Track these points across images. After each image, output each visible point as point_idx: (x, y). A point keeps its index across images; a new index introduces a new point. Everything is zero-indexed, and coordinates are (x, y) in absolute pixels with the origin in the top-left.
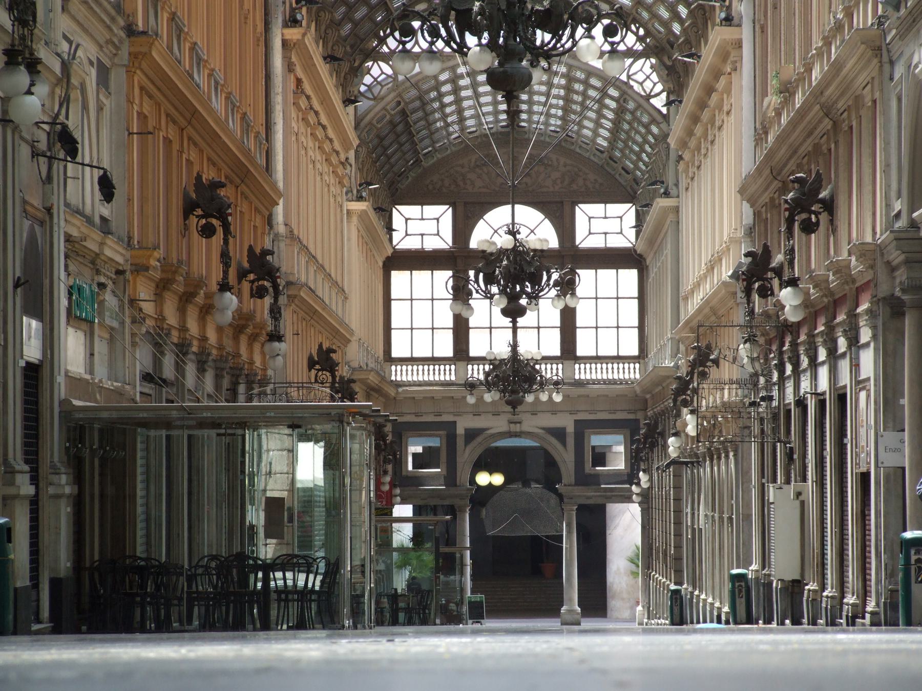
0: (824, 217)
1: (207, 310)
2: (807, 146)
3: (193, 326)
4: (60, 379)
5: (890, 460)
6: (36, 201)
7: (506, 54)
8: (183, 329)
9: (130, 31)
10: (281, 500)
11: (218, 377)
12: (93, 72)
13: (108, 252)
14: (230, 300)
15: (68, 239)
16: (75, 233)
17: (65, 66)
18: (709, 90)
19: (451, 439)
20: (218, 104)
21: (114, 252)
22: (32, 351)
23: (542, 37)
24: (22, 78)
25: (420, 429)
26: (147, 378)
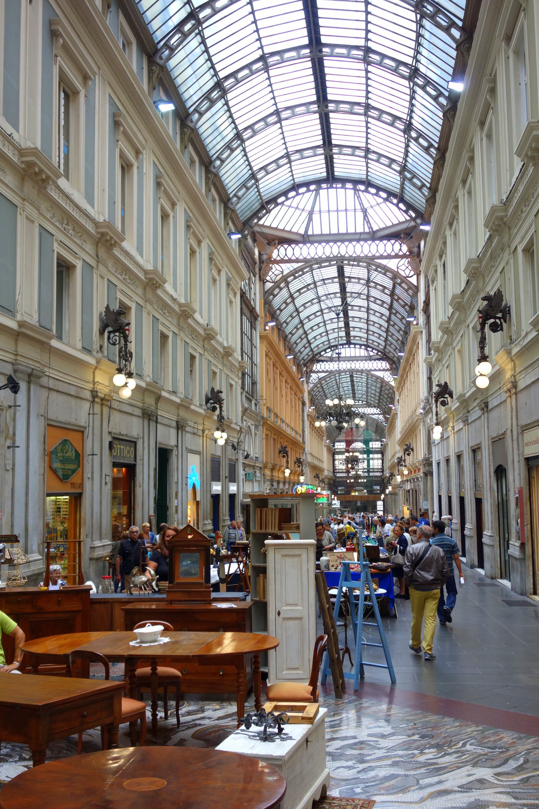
0: (412, 452)
7: (340, 422)
12: (253, 427)
17: (241, 428)
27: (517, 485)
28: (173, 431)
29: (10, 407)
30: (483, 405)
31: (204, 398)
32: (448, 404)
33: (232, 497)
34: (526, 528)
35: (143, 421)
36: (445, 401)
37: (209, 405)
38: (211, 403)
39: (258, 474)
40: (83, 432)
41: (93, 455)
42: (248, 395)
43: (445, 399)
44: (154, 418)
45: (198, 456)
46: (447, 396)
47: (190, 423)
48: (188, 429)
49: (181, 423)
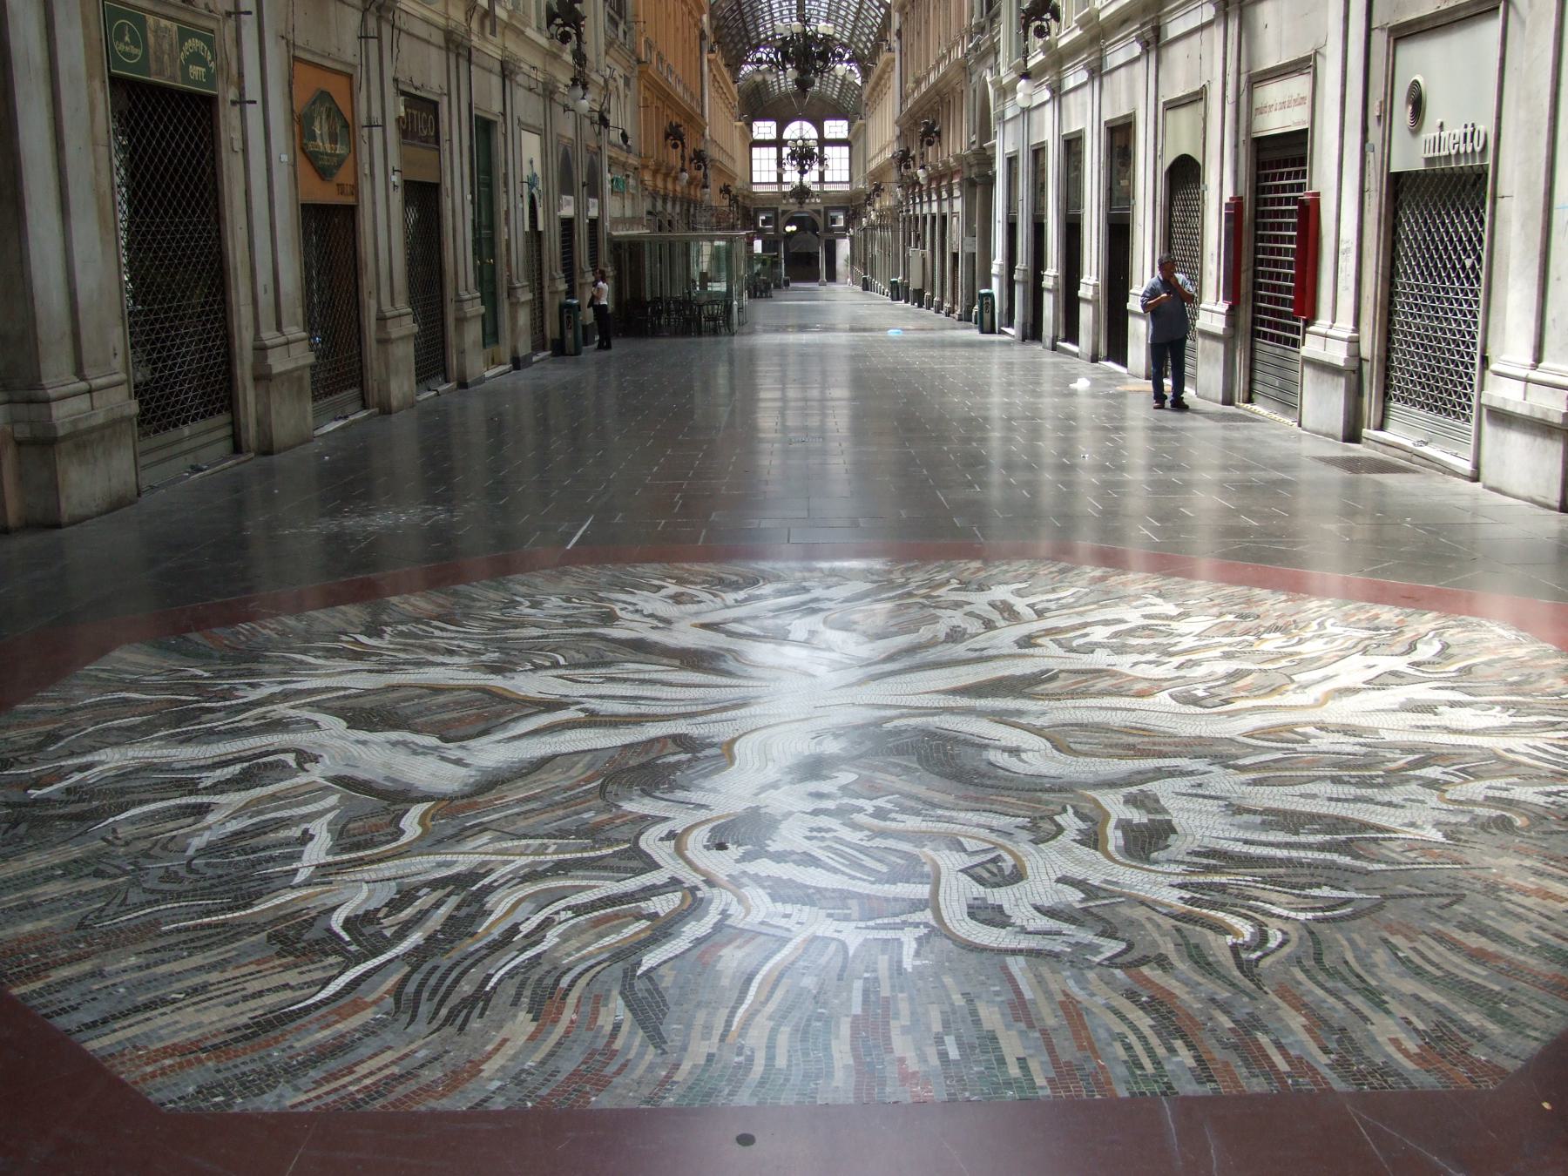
0: (936, 139)
1: (676, 179)
2: (928, 107)
3: (670, 186)
4: (607, 224)
5: (968, 249)
6: (593, 144)
8: (665, 188)
9: (639, 61)
10: (706, 274)
11: (681, 205)
13: (630, 161)
14: (686, 176)
15: (610, 158)
16: (613, 155)
17: (606, 81)
18: (880, 78)
19: (776, 214)
20: (680, 89)
21: (633, 160)
22: (593, 213)
23: (819, 64)
24: (580, 92)
25: (764, 210)
26: (649, 213)
27: (1228, 194)
28: (496, 81)
29: (229, 14)
30: (1149, 36)
31: (544, 14)
32: (1049, 33)
33: (594, 223)
34: (1243, 277)
35: (448, 59)
36: (1042, 27)
37: (553, 28)
38: (559, 26)
39: (631, 181)
40: (350, 76)
41: (370, 126)
42: (612, 12)
43: (1044, 24)
44: (466, 53)
45: (537, 137)
46: (1048, 16)
47: (526, 68)
48: (520, 78)
49: (511, 66)
